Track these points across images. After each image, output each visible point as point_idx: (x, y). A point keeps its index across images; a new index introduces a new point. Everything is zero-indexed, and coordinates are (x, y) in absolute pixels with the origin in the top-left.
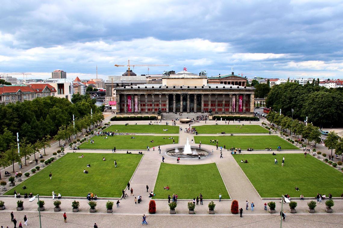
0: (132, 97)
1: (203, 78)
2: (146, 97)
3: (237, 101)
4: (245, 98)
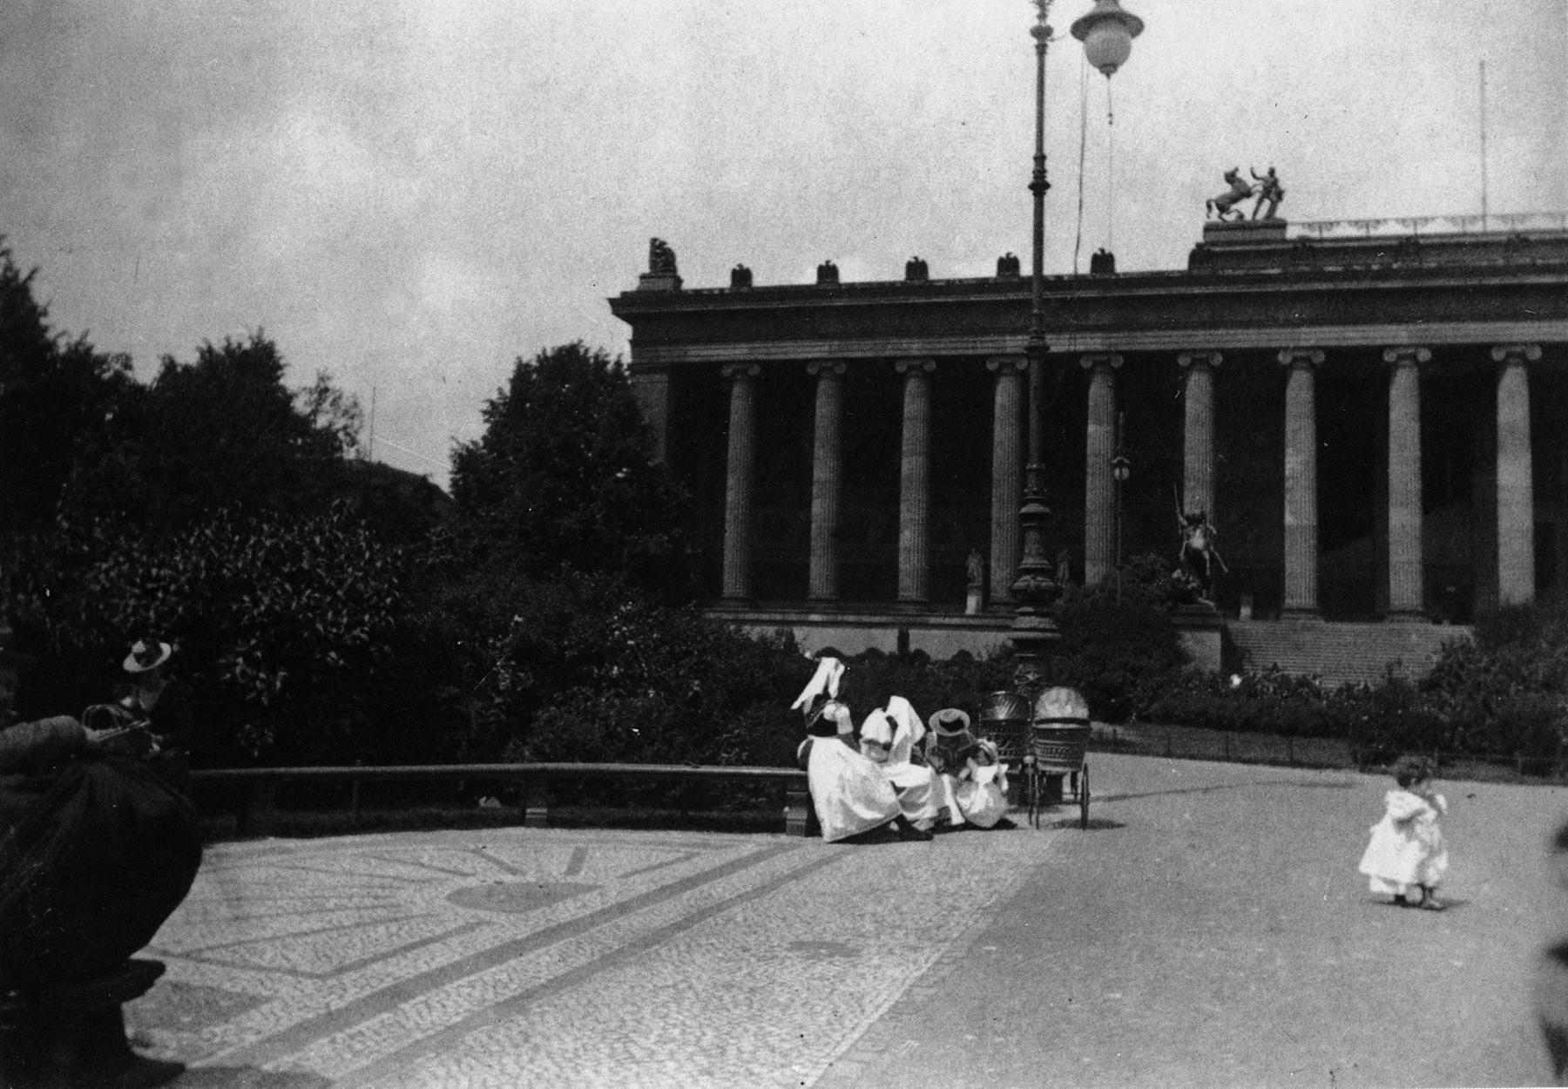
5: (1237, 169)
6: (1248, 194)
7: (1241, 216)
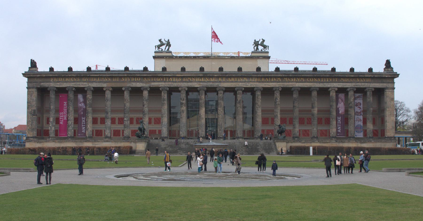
0: (71, 95)
1: (258, 57)
2: (108, 94)
3: (351, 107)
4: (370, 98)
5: (161, 39)
6: (164, 45)
7: (162, 50)
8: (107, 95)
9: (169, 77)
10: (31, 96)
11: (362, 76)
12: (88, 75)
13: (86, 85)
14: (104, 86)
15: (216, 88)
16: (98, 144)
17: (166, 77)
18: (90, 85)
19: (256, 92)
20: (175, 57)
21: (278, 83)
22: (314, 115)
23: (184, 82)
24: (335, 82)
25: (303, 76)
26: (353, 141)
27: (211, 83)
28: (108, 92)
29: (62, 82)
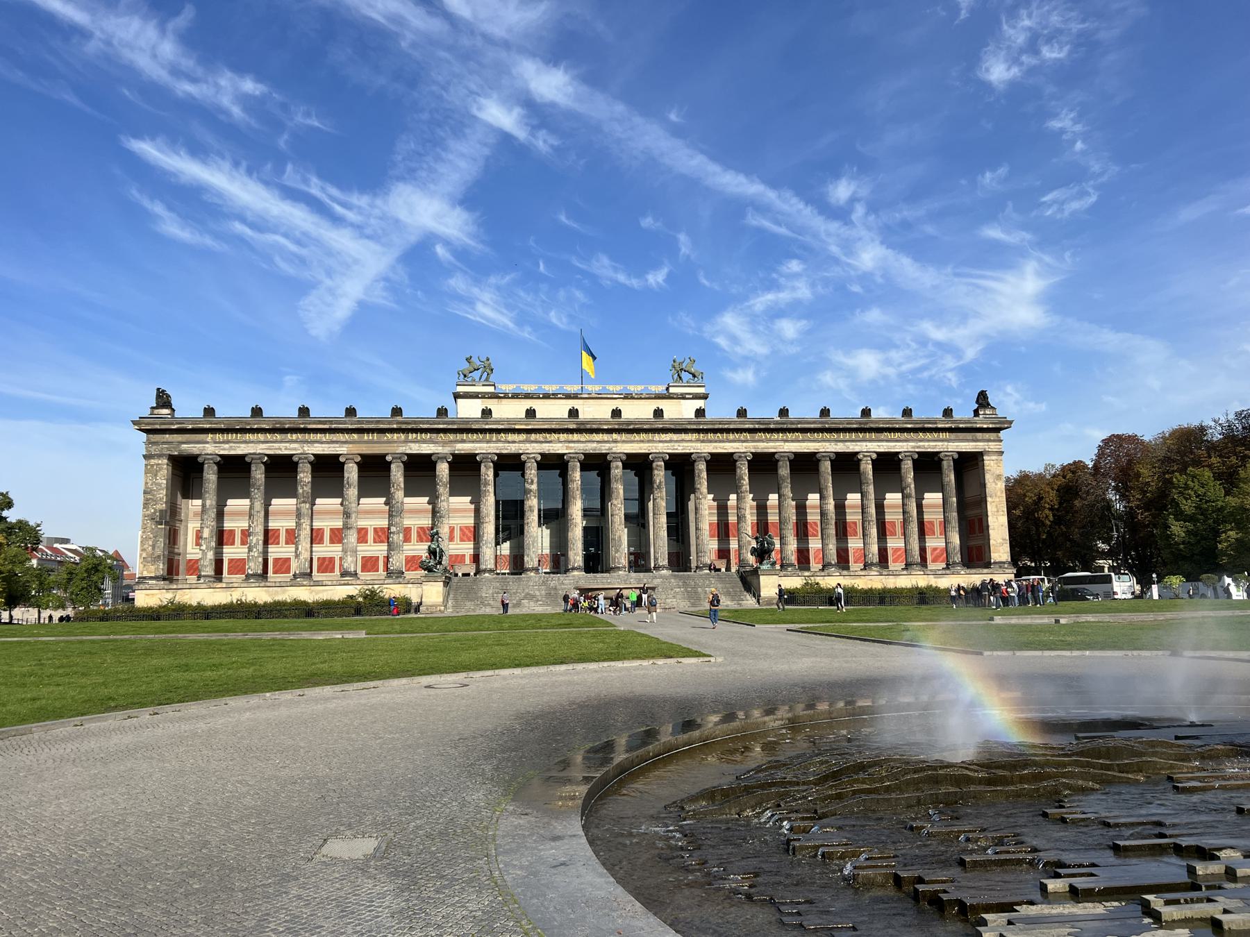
8: (351, 473)
9: (498, 431)
10: (156, 475)
11: (930, 426)
12: (302, 426)
13: (295, 449)
14: (341, 452)
15: (606, 454)
16: (327, 590)
17: (491, 431)
18: (306, 449)
19: (696, 464)
20: (502, 395)
21: (744, 444)
22: (827, 516)
23: (532, 442)
24: (871, 441)
25: (799, 426)
26: (919, 573)
27: (595, 445)
28: (351, 465)
29: (234, 443)
